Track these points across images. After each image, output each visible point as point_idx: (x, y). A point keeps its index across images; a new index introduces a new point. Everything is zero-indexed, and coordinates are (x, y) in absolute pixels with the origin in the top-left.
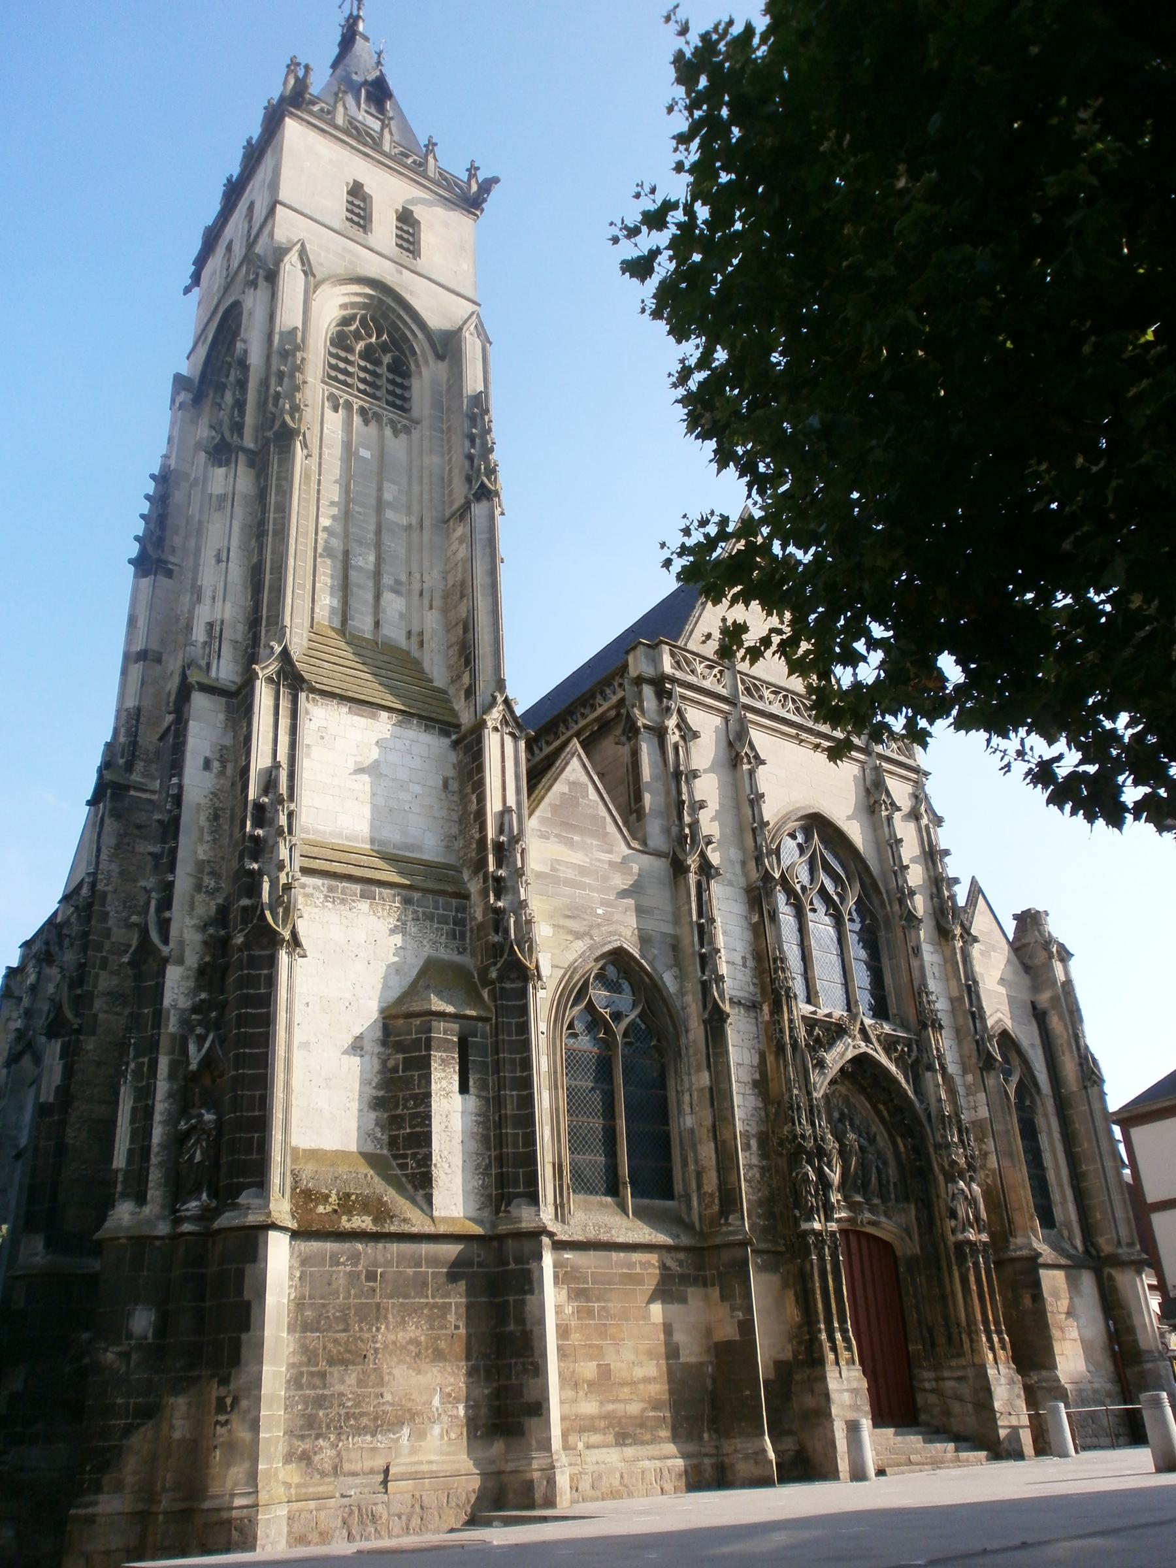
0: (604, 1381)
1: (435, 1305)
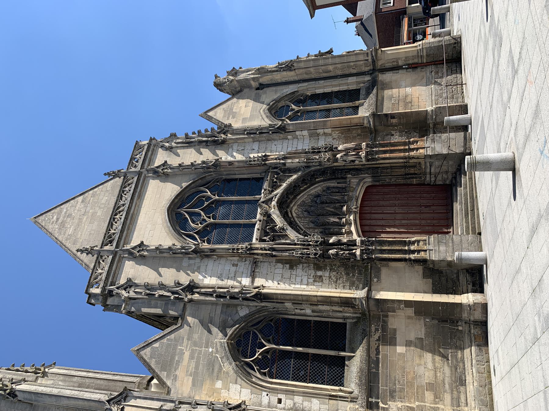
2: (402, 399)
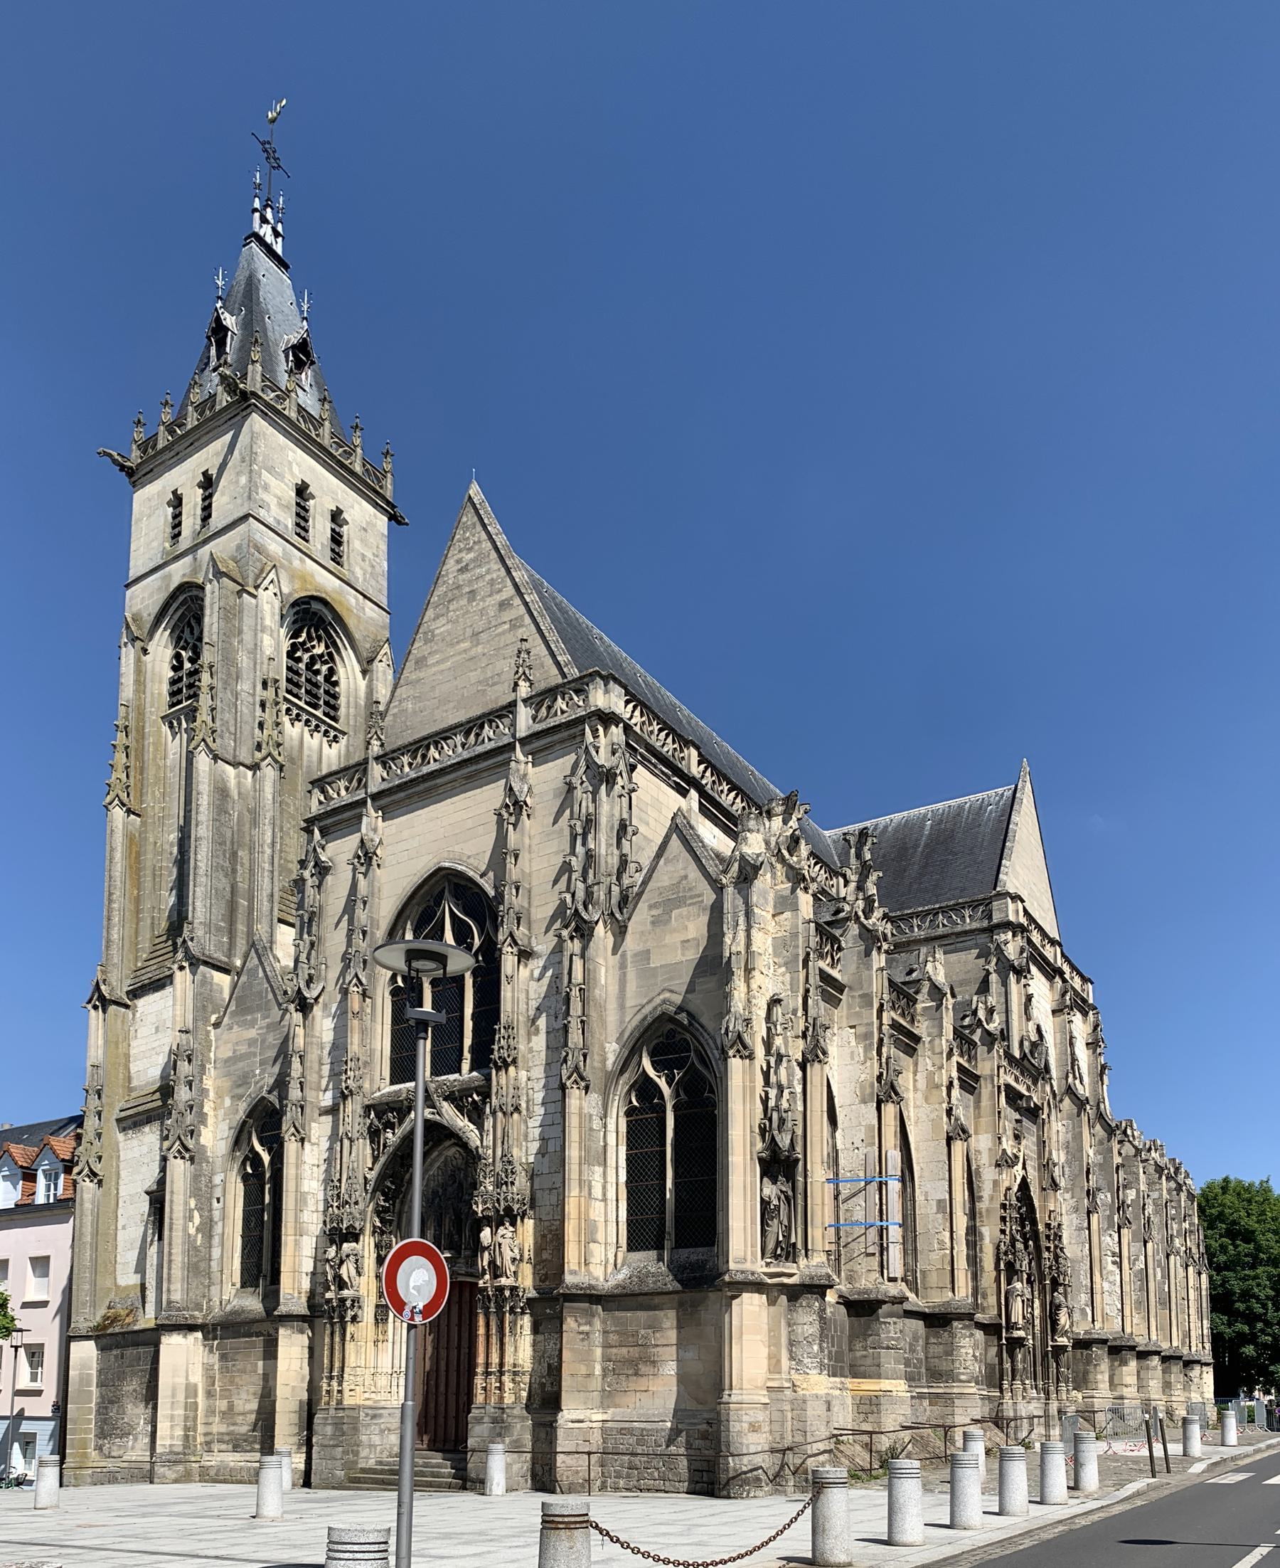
0: (229, 1414)
2: (221, 1368)
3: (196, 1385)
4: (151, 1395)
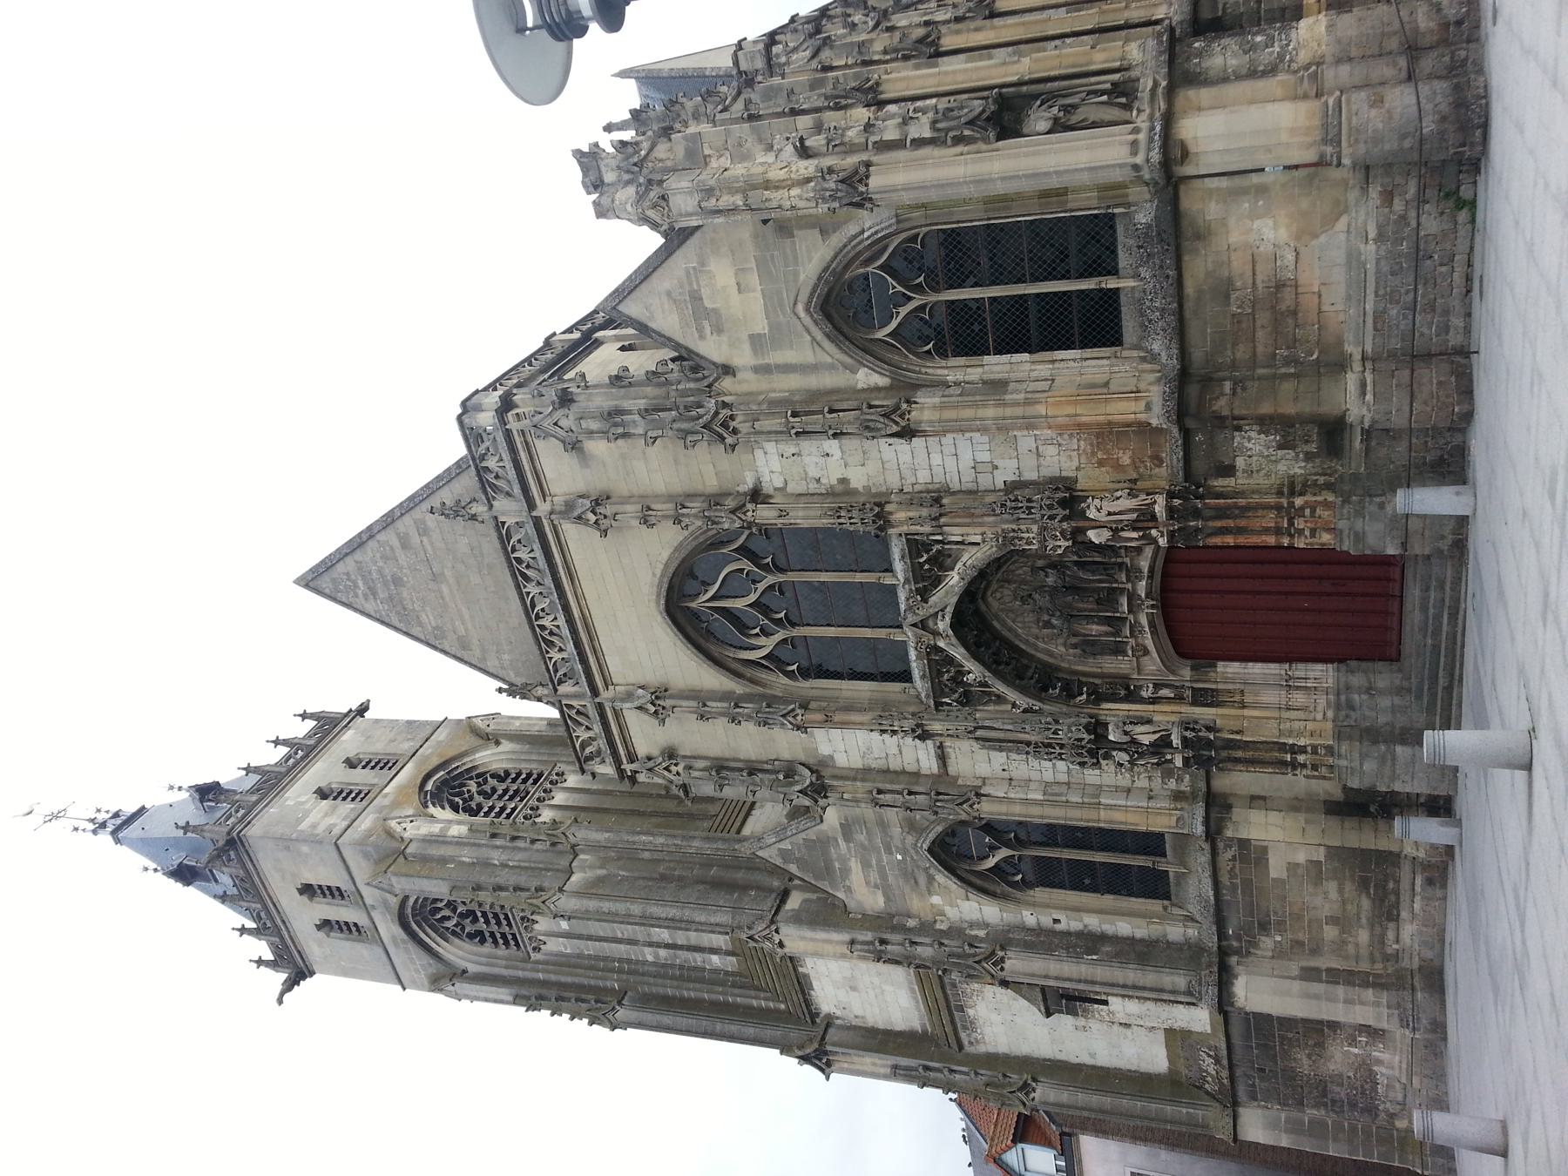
1: (1282, 1044)
2: (1281, 932)
3: (1303, 969)
4: (1318, 1031)
